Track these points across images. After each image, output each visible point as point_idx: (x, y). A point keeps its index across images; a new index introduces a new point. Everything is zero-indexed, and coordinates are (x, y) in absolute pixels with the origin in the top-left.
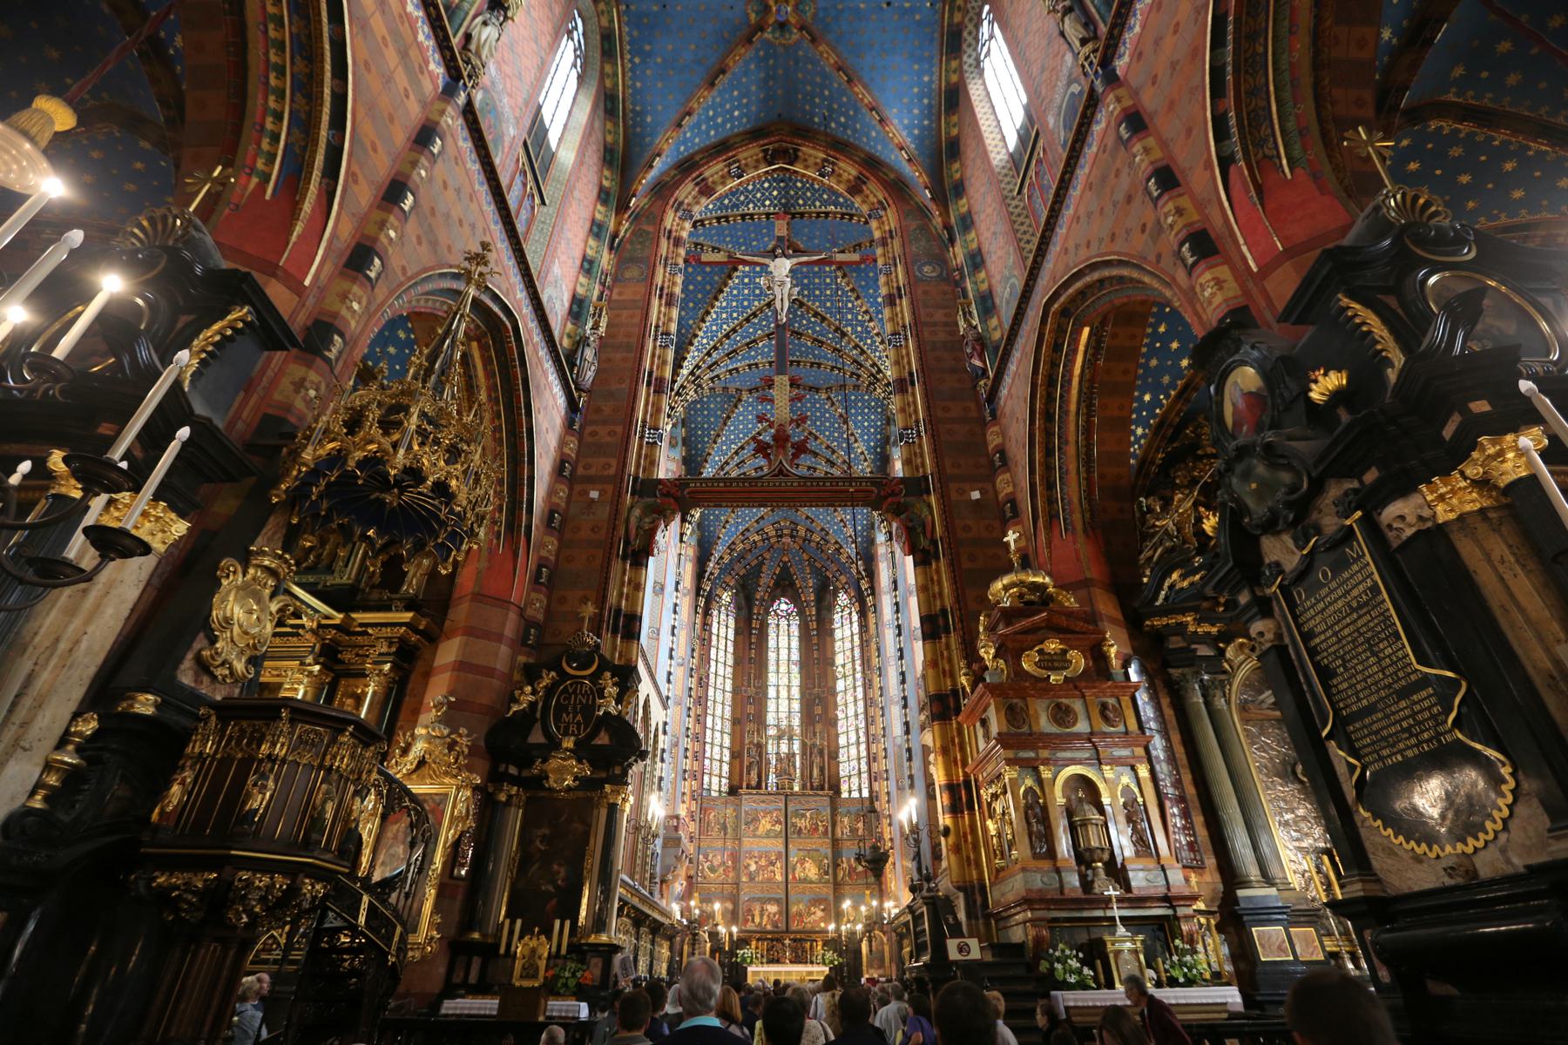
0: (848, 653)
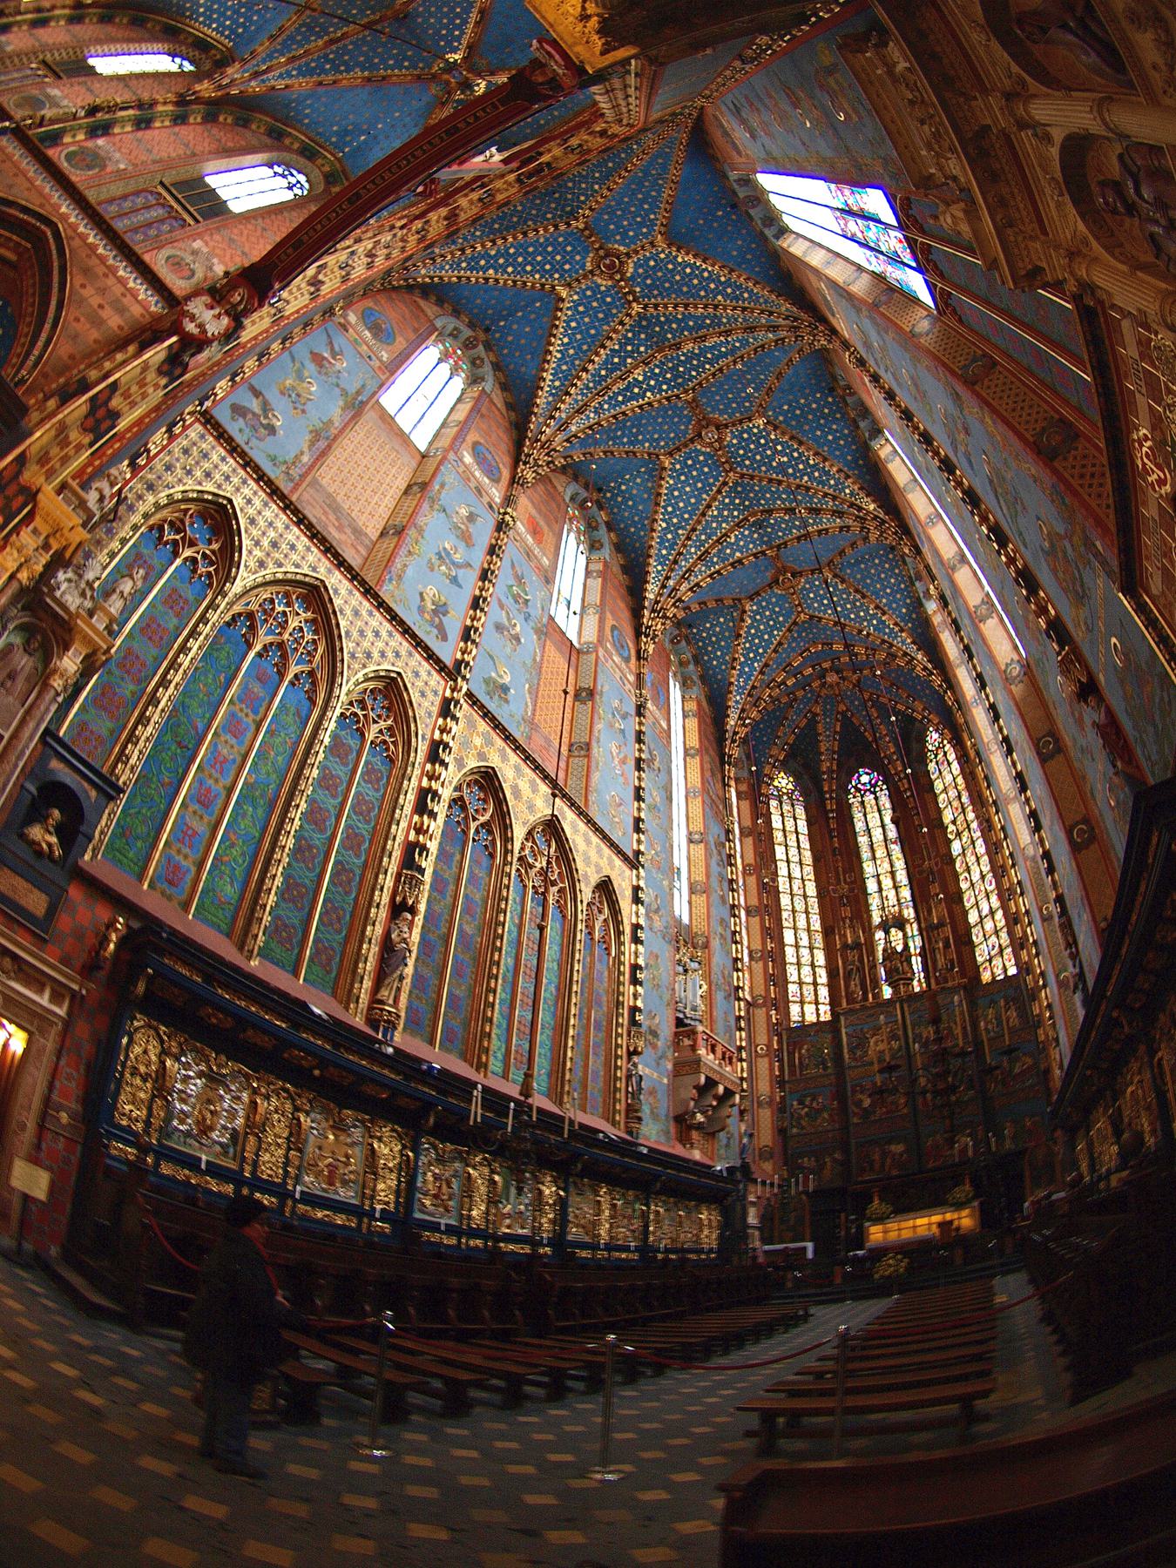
0: (956, 804)
